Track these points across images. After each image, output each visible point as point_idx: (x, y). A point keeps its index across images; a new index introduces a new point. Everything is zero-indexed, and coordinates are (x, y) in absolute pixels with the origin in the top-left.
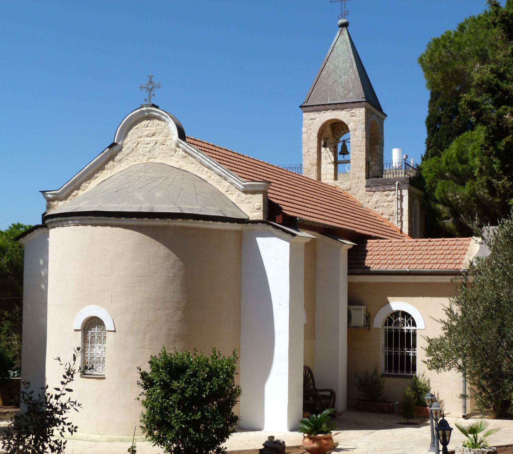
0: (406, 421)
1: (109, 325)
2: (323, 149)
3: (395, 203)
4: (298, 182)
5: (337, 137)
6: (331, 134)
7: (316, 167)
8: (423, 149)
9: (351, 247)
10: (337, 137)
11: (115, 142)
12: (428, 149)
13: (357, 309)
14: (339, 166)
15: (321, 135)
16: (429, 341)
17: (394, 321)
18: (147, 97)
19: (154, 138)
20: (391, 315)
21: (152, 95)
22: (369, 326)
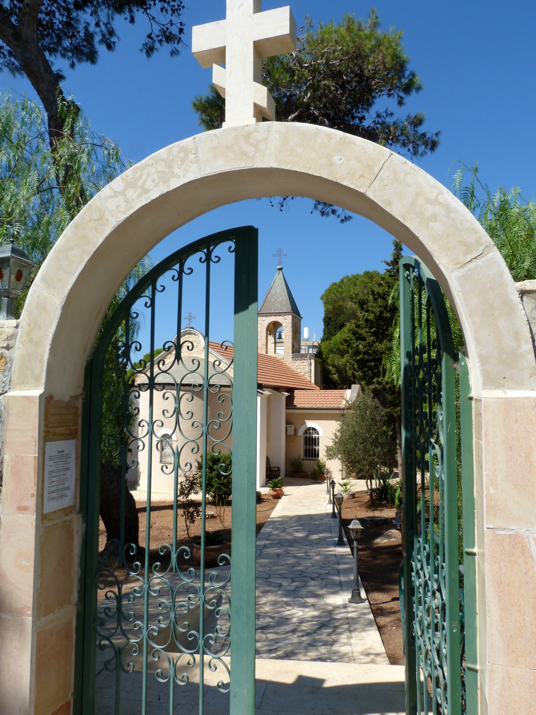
3: (307, 367)
8: (321, 334)
12: (325, 334)
14: (277, 345)
16: (327, 447)
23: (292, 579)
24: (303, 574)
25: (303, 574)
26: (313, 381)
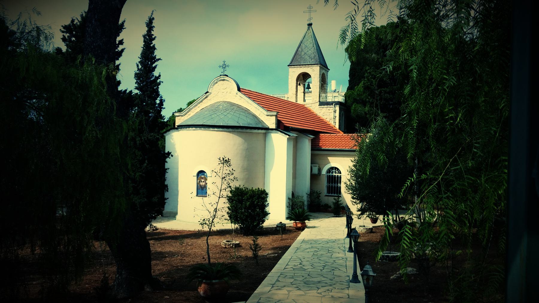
0: (336, 216)
2: (298, 86)
4: (288, 105)
6: (302, 78)
7: (295, 95)
9: (312, 138)
11: (208, 91)
15: (298, 79)
17: (331, 171)
18: (223, 71)
19: (226, 90)
21: (225, 70)
22: (320, 173)
26: (337, 126)
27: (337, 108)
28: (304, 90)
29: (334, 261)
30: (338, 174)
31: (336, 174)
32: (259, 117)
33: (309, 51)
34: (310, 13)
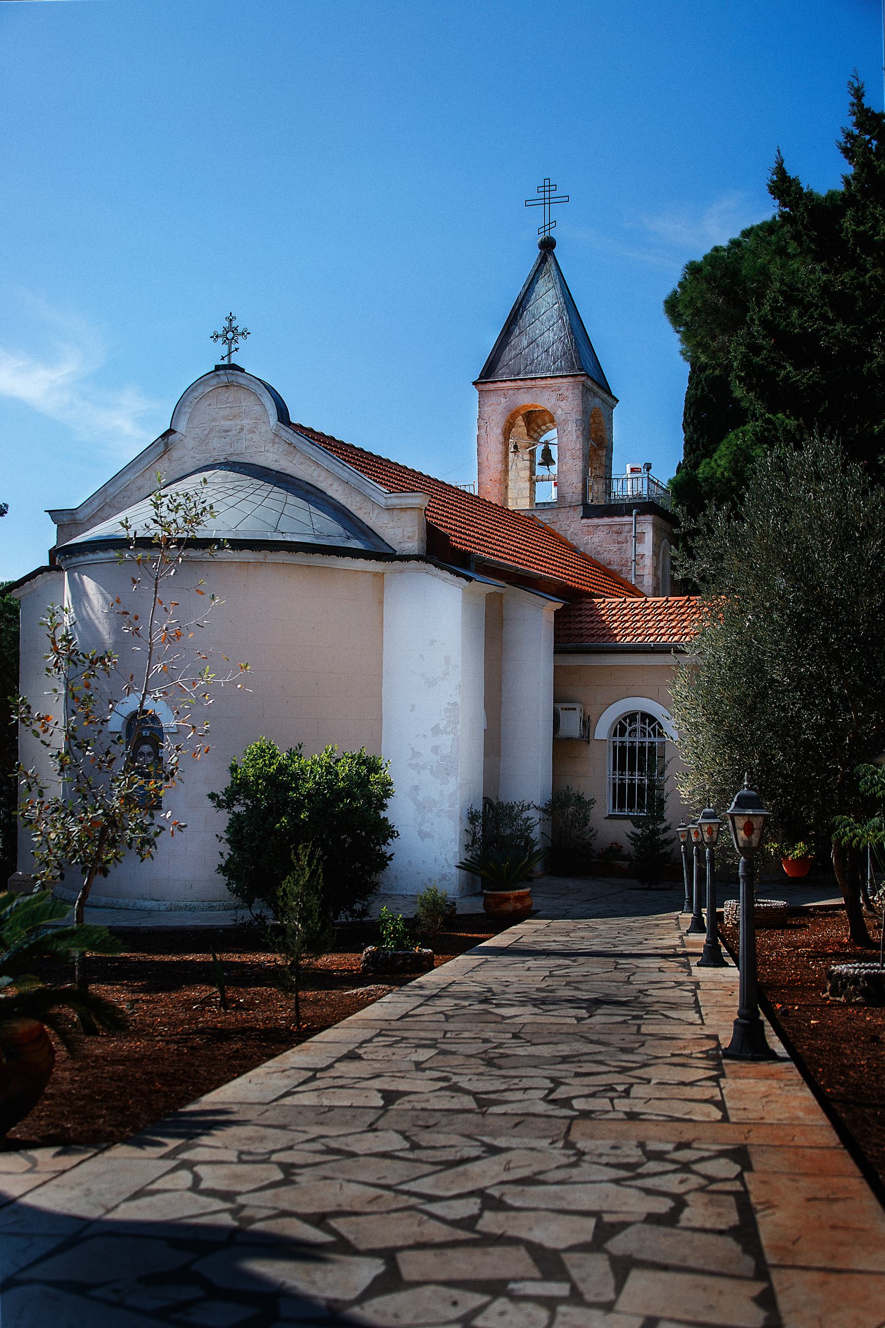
1: (168, 722)
2: (511, 455)
5: (535, 436)
10: (535, 436)
13: (569, 709)
17: (629, 729)
20: (625, 719)
23: (389, 1255)
24: (491, 1222)
25: (491, 1222)
27: (647, 527)
28: (533, 472)
29: (641, 991)
30: (652, 739)
31: (647, 739)
32: (360, 514)
33: (546, 334)
34: (547, 206)
